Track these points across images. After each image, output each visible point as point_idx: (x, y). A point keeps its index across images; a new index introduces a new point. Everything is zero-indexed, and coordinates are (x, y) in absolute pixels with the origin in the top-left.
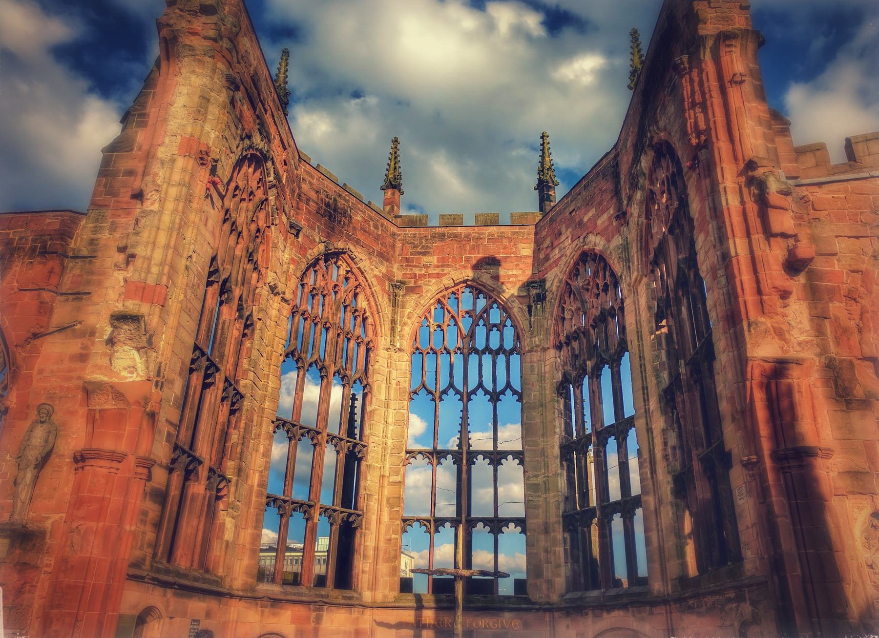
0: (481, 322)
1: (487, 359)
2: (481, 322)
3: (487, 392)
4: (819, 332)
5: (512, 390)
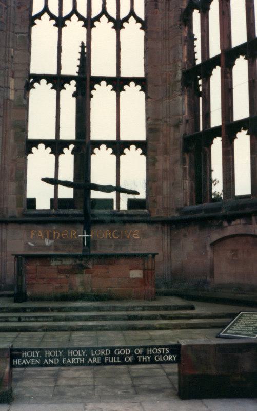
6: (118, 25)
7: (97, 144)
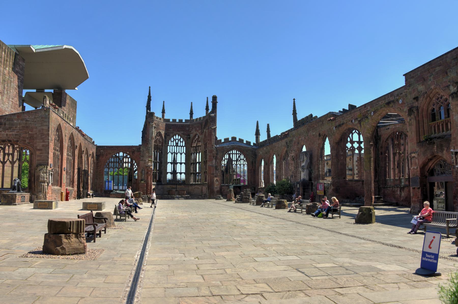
1: (180, 147)
3: (180, 153)
4: (215, 163)
6: (181, 154)
7: (178, 173)
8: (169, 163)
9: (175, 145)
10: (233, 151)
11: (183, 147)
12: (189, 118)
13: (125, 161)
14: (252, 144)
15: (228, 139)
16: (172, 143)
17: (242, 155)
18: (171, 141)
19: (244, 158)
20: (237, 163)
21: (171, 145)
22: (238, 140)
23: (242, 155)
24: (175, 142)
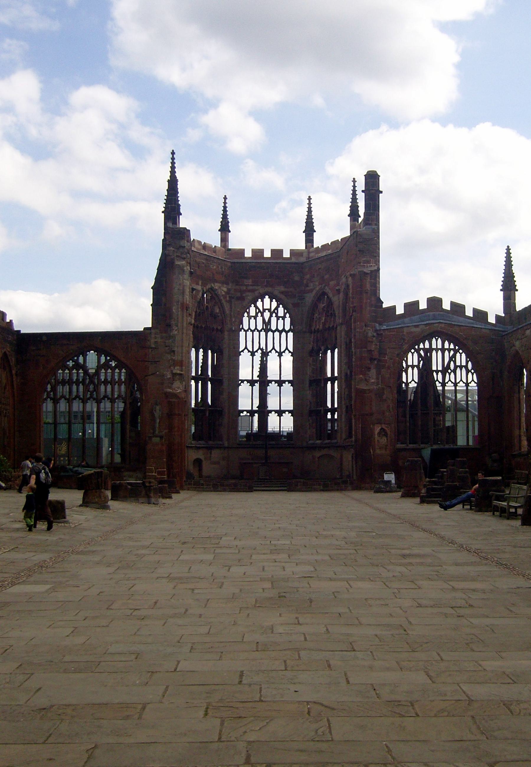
0: (274, 315)
1: (277, 334)
2: (274, 315)
4: (377, 378)
5: (289, 350)
6: (280, 354)
7: (271, 411)
8: (243, 381)
9: (263, 329)
10: (434, 340)
11: (287, 332)
12: (301, 245)
13: (103, 378)
14: (492, 320)
15: (417, 303)
16: (253, 321)
17: (461, 354)
18: (250, 317)
19: (467, 362)
20: (446, 381)
21: (249, 328)
22: (446, 306)
23: (461, 354)
24: (260, 319)
